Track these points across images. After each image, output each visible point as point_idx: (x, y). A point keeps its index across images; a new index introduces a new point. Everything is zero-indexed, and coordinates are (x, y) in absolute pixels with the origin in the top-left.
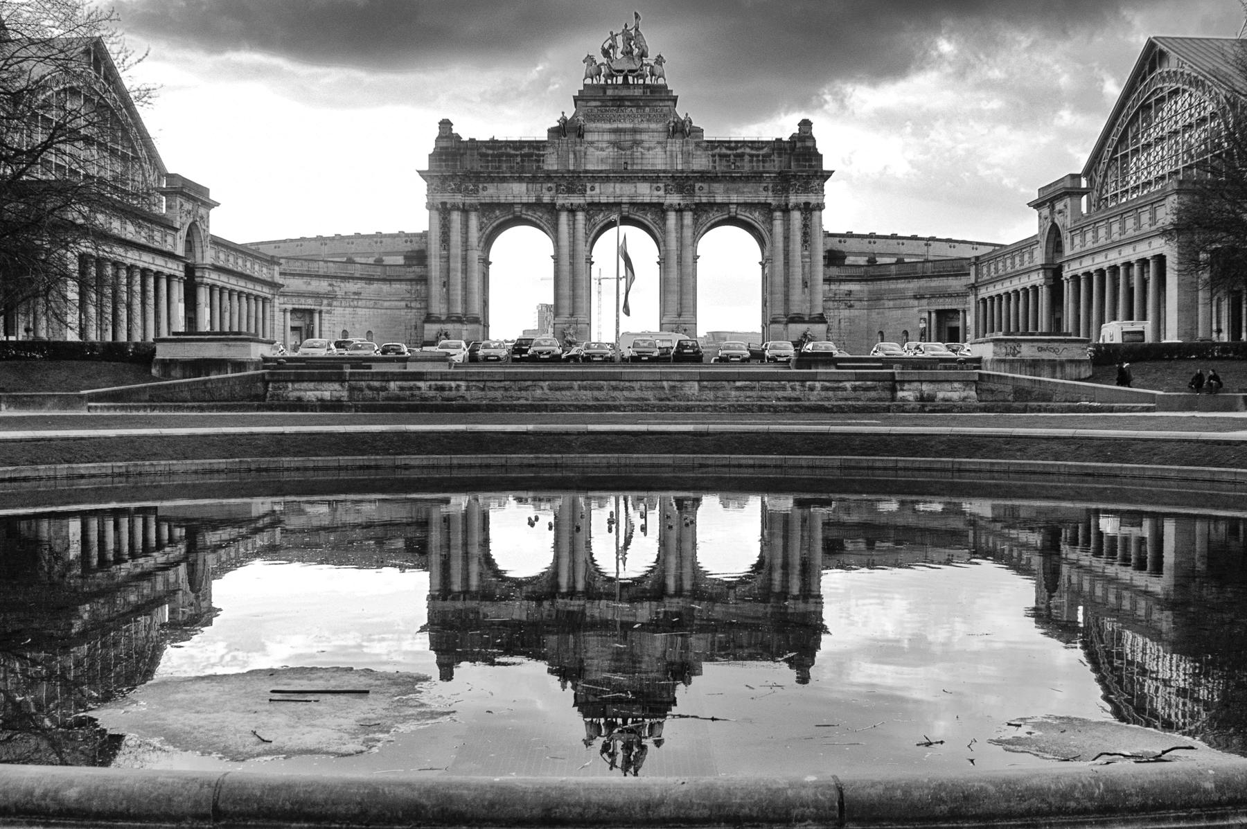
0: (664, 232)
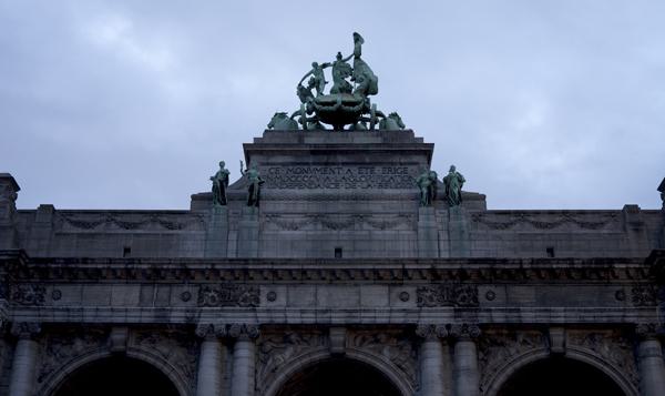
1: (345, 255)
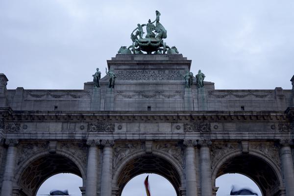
0: (184, 166)
1: (152, 109)
